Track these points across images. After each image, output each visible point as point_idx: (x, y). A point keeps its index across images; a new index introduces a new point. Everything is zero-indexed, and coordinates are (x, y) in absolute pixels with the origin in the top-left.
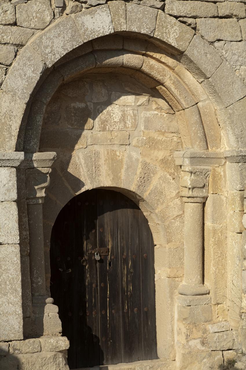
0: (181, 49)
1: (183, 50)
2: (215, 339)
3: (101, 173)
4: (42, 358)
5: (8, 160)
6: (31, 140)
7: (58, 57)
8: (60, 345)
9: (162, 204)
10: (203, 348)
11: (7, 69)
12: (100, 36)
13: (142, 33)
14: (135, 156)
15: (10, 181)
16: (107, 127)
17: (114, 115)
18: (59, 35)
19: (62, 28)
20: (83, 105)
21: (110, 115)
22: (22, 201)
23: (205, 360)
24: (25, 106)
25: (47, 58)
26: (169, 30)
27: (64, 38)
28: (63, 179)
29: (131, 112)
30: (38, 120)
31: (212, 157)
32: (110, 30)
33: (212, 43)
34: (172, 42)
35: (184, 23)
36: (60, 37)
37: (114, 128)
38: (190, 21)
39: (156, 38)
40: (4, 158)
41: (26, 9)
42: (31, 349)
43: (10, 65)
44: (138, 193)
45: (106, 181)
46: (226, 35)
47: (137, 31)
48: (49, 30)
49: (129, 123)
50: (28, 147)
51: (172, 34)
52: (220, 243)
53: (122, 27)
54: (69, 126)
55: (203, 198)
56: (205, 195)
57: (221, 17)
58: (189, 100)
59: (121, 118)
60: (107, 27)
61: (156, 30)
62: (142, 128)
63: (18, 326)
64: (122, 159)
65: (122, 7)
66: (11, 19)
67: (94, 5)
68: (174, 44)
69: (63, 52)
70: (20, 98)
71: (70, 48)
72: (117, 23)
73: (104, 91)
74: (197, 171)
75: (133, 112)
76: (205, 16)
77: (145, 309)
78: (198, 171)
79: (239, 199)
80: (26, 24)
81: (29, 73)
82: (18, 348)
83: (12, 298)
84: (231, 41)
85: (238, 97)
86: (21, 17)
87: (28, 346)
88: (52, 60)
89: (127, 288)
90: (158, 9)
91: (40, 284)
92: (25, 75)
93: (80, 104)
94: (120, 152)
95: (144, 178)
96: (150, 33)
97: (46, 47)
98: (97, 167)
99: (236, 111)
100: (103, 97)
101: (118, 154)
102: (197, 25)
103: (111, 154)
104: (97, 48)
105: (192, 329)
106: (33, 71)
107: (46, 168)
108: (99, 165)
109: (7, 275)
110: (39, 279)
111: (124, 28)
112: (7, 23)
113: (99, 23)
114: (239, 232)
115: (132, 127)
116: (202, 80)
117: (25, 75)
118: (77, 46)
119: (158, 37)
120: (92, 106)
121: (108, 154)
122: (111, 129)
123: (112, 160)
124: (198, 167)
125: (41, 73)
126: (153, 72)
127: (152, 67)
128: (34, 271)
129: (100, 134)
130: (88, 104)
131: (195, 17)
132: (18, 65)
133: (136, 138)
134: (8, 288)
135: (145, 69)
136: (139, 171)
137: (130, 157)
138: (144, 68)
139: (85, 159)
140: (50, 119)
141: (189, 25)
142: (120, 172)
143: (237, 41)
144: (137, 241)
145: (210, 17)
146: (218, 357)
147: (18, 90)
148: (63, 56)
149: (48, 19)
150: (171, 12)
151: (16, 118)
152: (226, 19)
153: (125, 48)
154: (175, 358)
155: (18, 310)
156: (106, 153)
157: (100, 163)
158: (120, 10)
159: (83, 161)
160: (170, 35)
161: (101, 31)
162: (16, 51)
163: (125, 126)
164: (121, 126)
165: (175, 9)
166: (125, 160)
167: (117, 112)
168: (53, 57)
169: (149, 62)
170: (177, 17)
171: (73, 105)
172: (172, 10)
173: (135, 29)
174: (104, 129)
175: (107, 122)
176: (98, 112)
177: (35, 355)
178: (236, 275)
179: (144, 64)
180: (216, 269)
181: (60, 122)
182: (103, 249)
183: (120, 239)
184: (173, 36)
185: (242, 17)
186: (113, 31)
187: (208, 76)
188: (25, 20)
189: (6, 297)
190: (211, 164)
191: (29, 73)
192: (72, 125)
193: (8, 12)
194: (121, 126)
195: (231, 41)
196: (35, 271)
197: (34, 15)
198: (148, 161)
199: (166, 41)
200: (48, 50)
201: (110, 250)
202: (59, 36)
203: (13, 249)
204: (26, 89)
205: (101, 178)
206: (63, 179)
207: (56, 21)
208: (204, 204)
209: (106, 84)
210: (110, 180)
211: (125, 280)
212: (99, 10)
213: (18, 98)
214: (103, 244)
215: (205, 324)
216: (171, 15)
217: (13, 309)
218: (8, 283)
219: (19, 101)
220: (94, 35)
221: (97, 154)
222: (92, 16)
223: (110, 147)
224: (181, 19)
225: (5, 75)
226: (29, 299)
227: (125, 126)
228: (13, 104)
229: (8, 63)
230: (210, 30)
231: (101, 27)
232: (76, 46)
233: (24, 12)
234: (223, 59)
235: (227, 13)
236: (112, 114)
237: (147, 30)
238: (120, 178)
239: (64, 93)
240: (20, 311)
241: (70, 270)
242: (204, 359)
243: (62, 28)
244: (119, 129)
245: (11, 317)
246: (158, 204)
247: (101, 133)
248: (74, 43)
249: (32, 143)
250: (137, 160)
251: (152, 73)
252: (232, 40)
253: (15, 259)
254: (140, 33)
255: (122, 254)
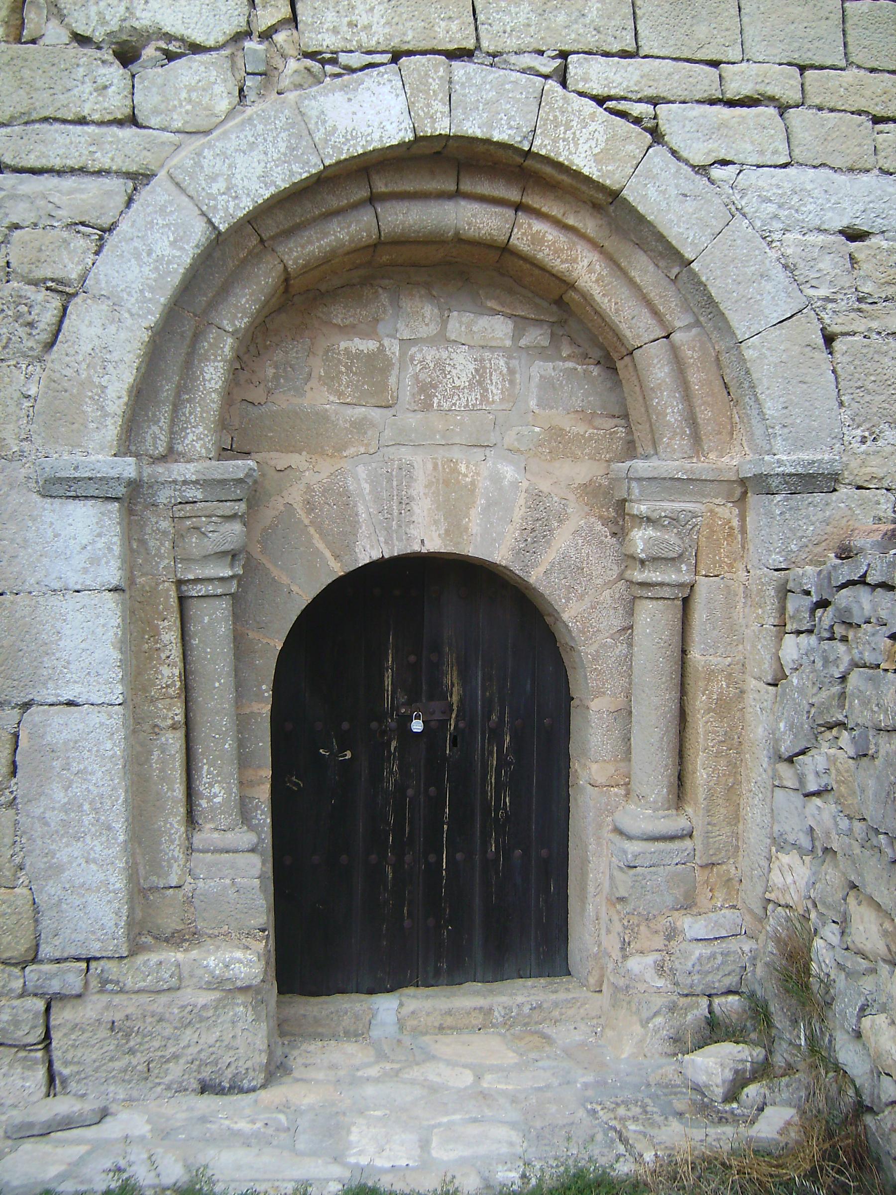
0: (608, 182)
1: (616, 187)
2: (690, 964)
3: (414, 518)
4: (183, 1007)
5: (90, 479)
6: (187, 428)
7: (247, 205)
8: (234, 974)
9: (581, 598)
10: (660, 983)
11: (101, 238)
12: (371, 148)
13: (495, 140)
14: (508, 476)
15: (100, 535)
16: (436, 400)
17: (454, 372)
18: (252, 146)
19: (260, 127)
20: (370, 345)
21: (444, 370)
22: (161, 587)
23: (659, 1020)
24: (146, 336)
25: (215, 207)
26: (574, 133)
27: (266, 153)
28: (312, 530)
29: (502, 363)
30: (208, 377)
31: (703, 478)
32: (402, 134)
33: (701, 170)
34: (583, 162)
35: (623, 114)
36: (255, 153)
37: (455, 404)
38: (638, 109)
39: (537, 154)
40: (77, 475)
41: (160, 81)
42: (152, 981)
43: (110, 230)
44: (517, 569)
45: (428, 537)
46: (744, 150)
47: (479, 134)
48: (225, 133)
49: (495, 391)
50: (180, 448)
51: (584, 143)
52: (728, 707)
53: (436, 125)
54: (332, 398)
55: (681, 585)
56: (687, 578)
57: (731, 103)
58: (641, 325)
59: (474, 377)
60: (394, 125)
61: (538, 131)
62: (533, 404)
63: (114, 922)
64: (473, 483)
65: (436, 72)
66: (119, 108)
67: (355, 66)
68: (589, 169)
69: (261, 191)
70: (132, 315)
71: (283, 180)
72: (421, 113)
73: (429, 310)
74: (663, 514)
75: (506, 363)
76: (682, 98)
77: (544, 853)
78: (666, 517)
79: (773, 593)
80: (159, 119)
81: (163, 246)
82: (115, 978)
83: (98, 848)
84: (758, 166)
85: (775, 315)
86: (146, 103)
87: (142, 972)
88: (230, 210)
89: (498, 800)
90: (546, 77)
91: (216, 800)
92: (149, 254)
93: (365, 341)
94: (467, 466)
95: (533, 530)
96: (520, 142)
97: (213, 178)
98: (405, 503)
99: (768, 353)
100: (427, 325)
101: (463, 469)
102: (660, 122)
103: (444, 468)
104: (383, 189)
105: (638, 925)
106: (175, 241)
107: (228, 504)
108: (410, 498)
109: (84, 787)
110: (216, 789)
111: (442, 127)
112: (109, 117)
113: (373, 115)
114: (770, 681)
115: (502, 400)
116: (675, 271)
117: (149, 254)
118: (305, 176)
119: (543, 152)
120: (396, 349)
121: (435, 467)
122: (446, 406)
123: (446, 483)
124: (666, 505)
125: (197, 246)
126: (540, 251)
127: (537, 239)
128: (202, 768)
129: (413, 420)
130: (386, 342)
131: (655, 101)
132: (132, 226)
133: (516, 429)
134: (86, 820)
135: (520, 241)
136: (518, 513)
137: (496, 478)
138: (516, 242)
139: (372, 481)
140: (282, 381)
141: (637, 121)
142: (467, 515)
143: (775, 167)
144: (529, 686)
145: (698, 102)
146: (695, 1012)
147: (130, 294)
148: (261, 201)
149: (223, 105)
150: (580, 87)
151: (122, 366)
152: (745, 109)
153: (467, 186)
154: (601, 985)
155: (112, 880)
156: (430, 466)
157: (414, 493)
158: (430, 80)
159: (366, 487)
160: (576, 145)
161: (376, 136)
162: (129, 191)
163: (484, 397)
164: (473, 397)
165: (594, 78)
166: (483, 484)
167: (464, 362)
168: (232, 204)
169: (529, 224)
170: (600, 101)
171: (343, 345)
172: (586, 80)
173: (473, 128)
174: (427, 407)
175: (435, 387)
176: (412, 363)
177: (163, 999)
178: (760, 795)
179: (515, 230)
180: (709, 775)
181: (307, 388)
182: (436, 705)
183: (483, 679)
184: (586, 147)
185: (791, 102)
186: (410, 136)
187: (689, 256)
188: (156, 111)
189: (80, 844)
190: (703, 496)
191: (163, 246)
192: (340, 394)
193: (111, 90)
194: (473, 397)
195: (758, 166)
196: (206, 767)
197: (184, 95)
198: (545, 486)
199: (566, 163)
200: (221, 185)
201: (455, 707)
202: (252, 150)
203: (103, 718)
204: (152, 289)
205: (414, 531)
206: (312, 530)
207: (249, 111)
208: (686, 601)
209: (434, 293)
210: (439, 535)
211: (493, 781)
212: (370, 78)
213: (127, 315)
214: (438, 692)
215: (676, 914)
216: (581, 94)
217: (101, 876)
218: (86, 807)
219: (129, 322)
220: (354, 146)
221: (407, 472)
222: (351, 96)
223: (441, 453)
224: (610, 104)
225: (97, 253)
226: (177, 842)
227: (484, 397)
228: (112, 329)
229: (105, 222)
230: (696, 135)
231: (376, 124)
232: (301, 174)
233: (154, 90)
234: (736, 212)
235: (747, 89)
236: (448, 368)
237: (510, 132)
238: (466, 529)
239: (321, 315)
240: (118, 882)
241: (349, 754)
242: (655, 1014)
243: (260, 127)
244: (467, 405)
245: (92, 898)
246: (568, 599)
247: (420, 415)
248: (296, 168)
249: (191, 437)
250: (515, 485)
251: (540, 256)
252: (760, 163)
253: (109, 745)
254: (488, 142)
255: (487, 716)
